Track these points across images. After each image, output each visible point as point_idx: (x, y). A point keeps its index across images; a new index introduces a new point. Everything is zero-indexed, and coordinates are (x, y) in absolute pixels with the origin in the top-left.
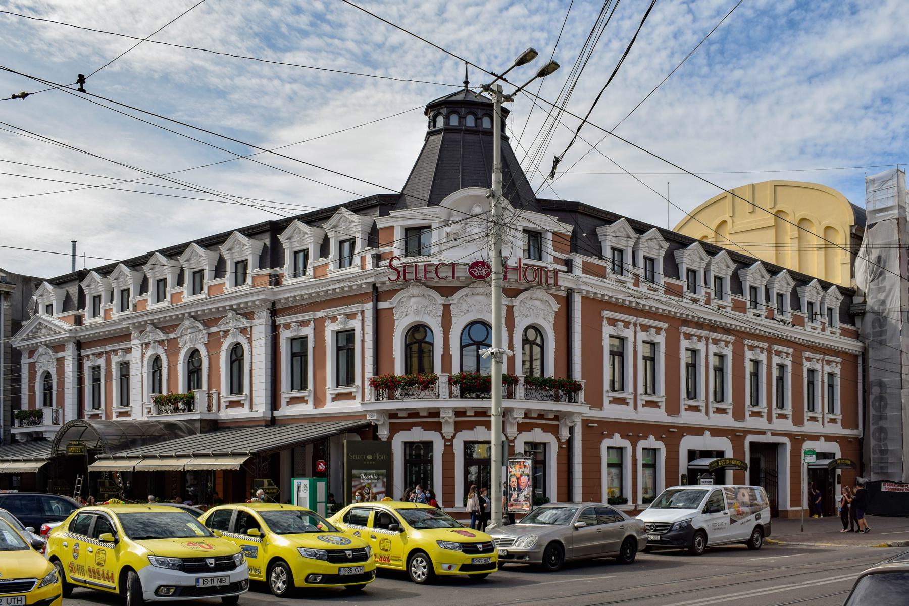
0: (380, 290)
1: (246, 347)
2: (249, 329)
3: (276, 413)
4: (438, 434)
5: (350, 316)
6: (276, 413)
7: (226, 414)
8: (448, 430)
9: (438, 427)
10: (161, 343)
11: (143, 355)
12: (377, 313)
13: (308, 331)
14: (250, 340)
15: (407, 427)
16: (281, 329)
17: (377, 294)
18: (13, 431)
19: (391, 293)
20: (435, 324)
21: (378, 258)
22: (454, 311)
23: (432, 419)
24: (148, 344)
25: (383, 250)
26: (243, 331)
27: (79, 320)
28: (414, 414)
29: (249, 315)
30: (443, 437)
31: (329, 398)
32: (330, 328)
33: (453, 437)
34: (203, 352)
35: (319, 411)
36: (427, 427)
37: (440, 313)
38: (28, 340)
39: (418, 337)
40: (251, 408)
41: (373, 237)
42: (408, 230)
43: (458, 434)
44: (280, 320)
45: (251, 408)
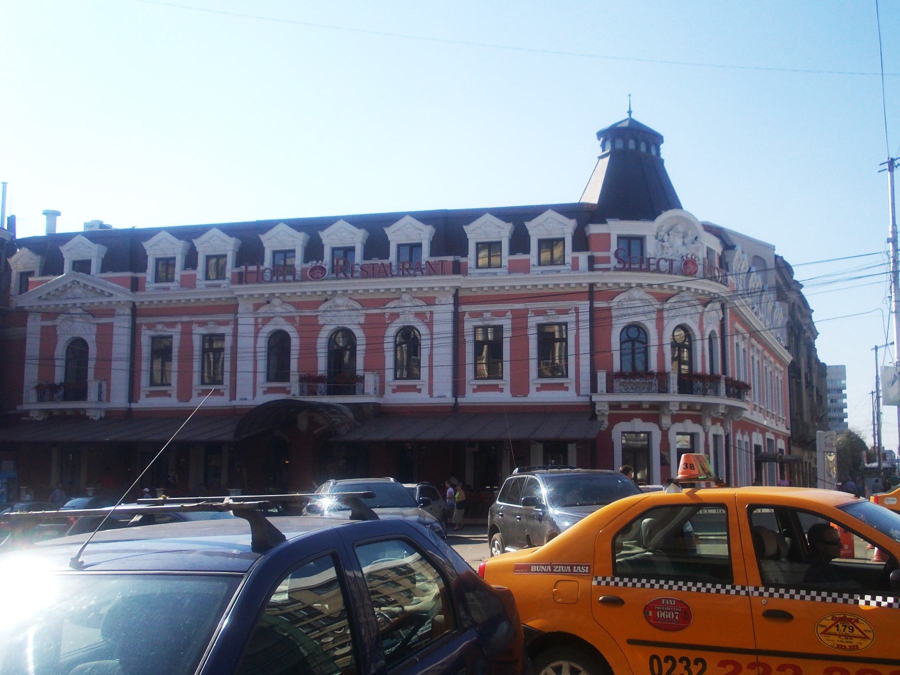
0: (595, 289)
1: (423, 329)
2: (428, 315)
3: (460, 400)
4: (655, 425)
5: (565, 312)
6: (460, 400)
7: (394, 398)
8: (666, 421)
9: (656, 419)
10: (290, 319)
11: (257, 332)
12: (592, 310)
13: (506, 323)
14: (430, 325)
15: (628, 418)
16: (467, 316)
17: (592, 293)
18: (26, 407)
19: (610, 295)
20: (651, 327)
21: (592, 261)
22: (665, 314)
23: (654, 413)
24: (267, 320)
25: (598, 254)
26: (420, 315)
27: (136, 285)
28: (637, 406)
29: (430, 301)
30: (661, 428)
31: (533, 388)
32: (533, 321)
33: (669, 429)
34: (359, 333)
35: (520, 400)
36: (646, 418)
37: (654, 316)
38: (45, 299)
39: (635, 337)
40: (431, 392)
41: (581, 242)
42: (620, 238)
43: (673, 426)
44: (463, 308)
45: (431, 392)
